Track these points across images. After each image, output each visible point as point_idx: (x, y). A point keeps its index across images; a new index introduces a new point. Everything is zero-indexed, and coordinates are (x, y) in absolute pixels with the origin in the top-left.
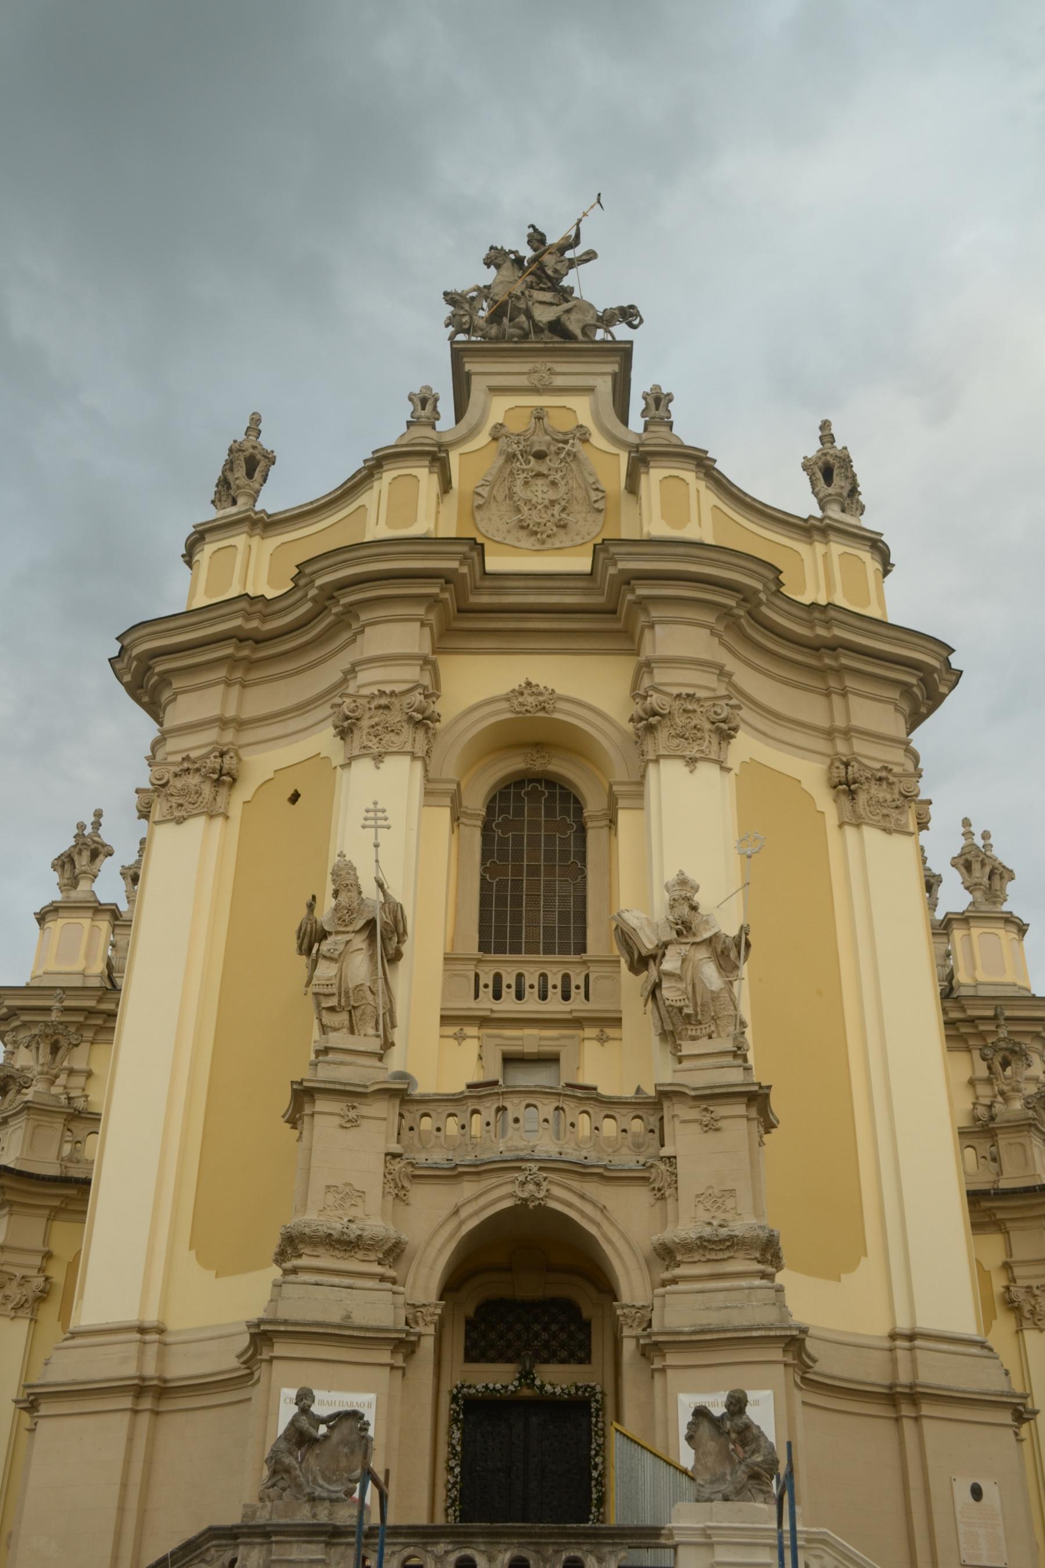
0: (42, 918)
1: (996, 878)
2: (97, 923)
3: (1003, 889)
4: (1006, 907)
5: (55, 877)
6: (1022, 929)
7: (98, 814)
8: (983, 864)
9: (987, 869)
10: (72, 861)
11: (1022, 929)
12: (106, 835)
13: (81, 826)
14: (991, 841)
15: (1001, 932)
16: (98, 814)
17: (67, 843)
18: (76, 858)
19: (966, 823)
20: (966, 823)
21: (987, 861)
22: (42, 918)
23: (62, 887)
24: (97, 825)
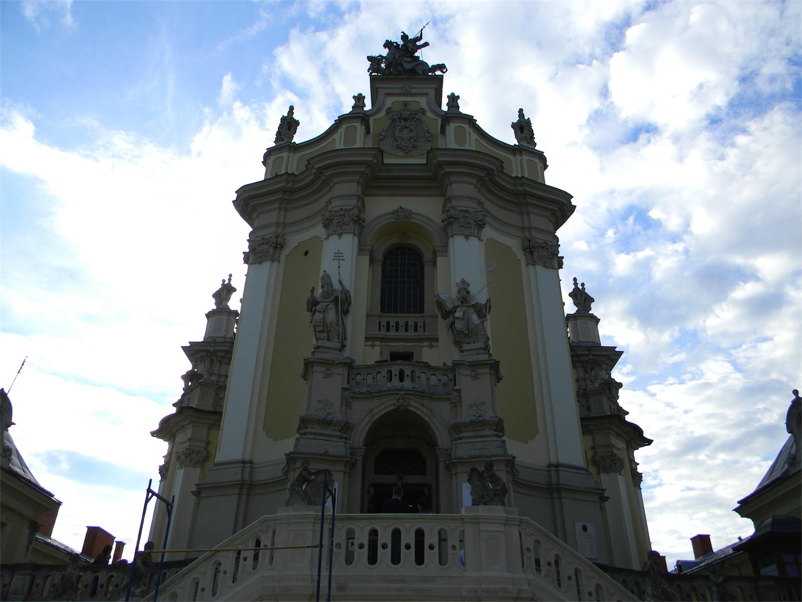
0: (208, 316)
1: (587, 301)
2: (230, 318)
4: (590, 312)
5: (214, 300)
6: (598, 320)
7: (230, 276)
8: (582, 295)
9: (583, 298)
11: (598, 320)
12: (233, 284)
13: (224, 281)
15: (589, 322)
16: (230, 276)
17: (218, 286)
18: (222, 293)
19: (575, 279)
20: (575, 279)
21: (583, 294)
23: (216, 304)
24: (230, 280)
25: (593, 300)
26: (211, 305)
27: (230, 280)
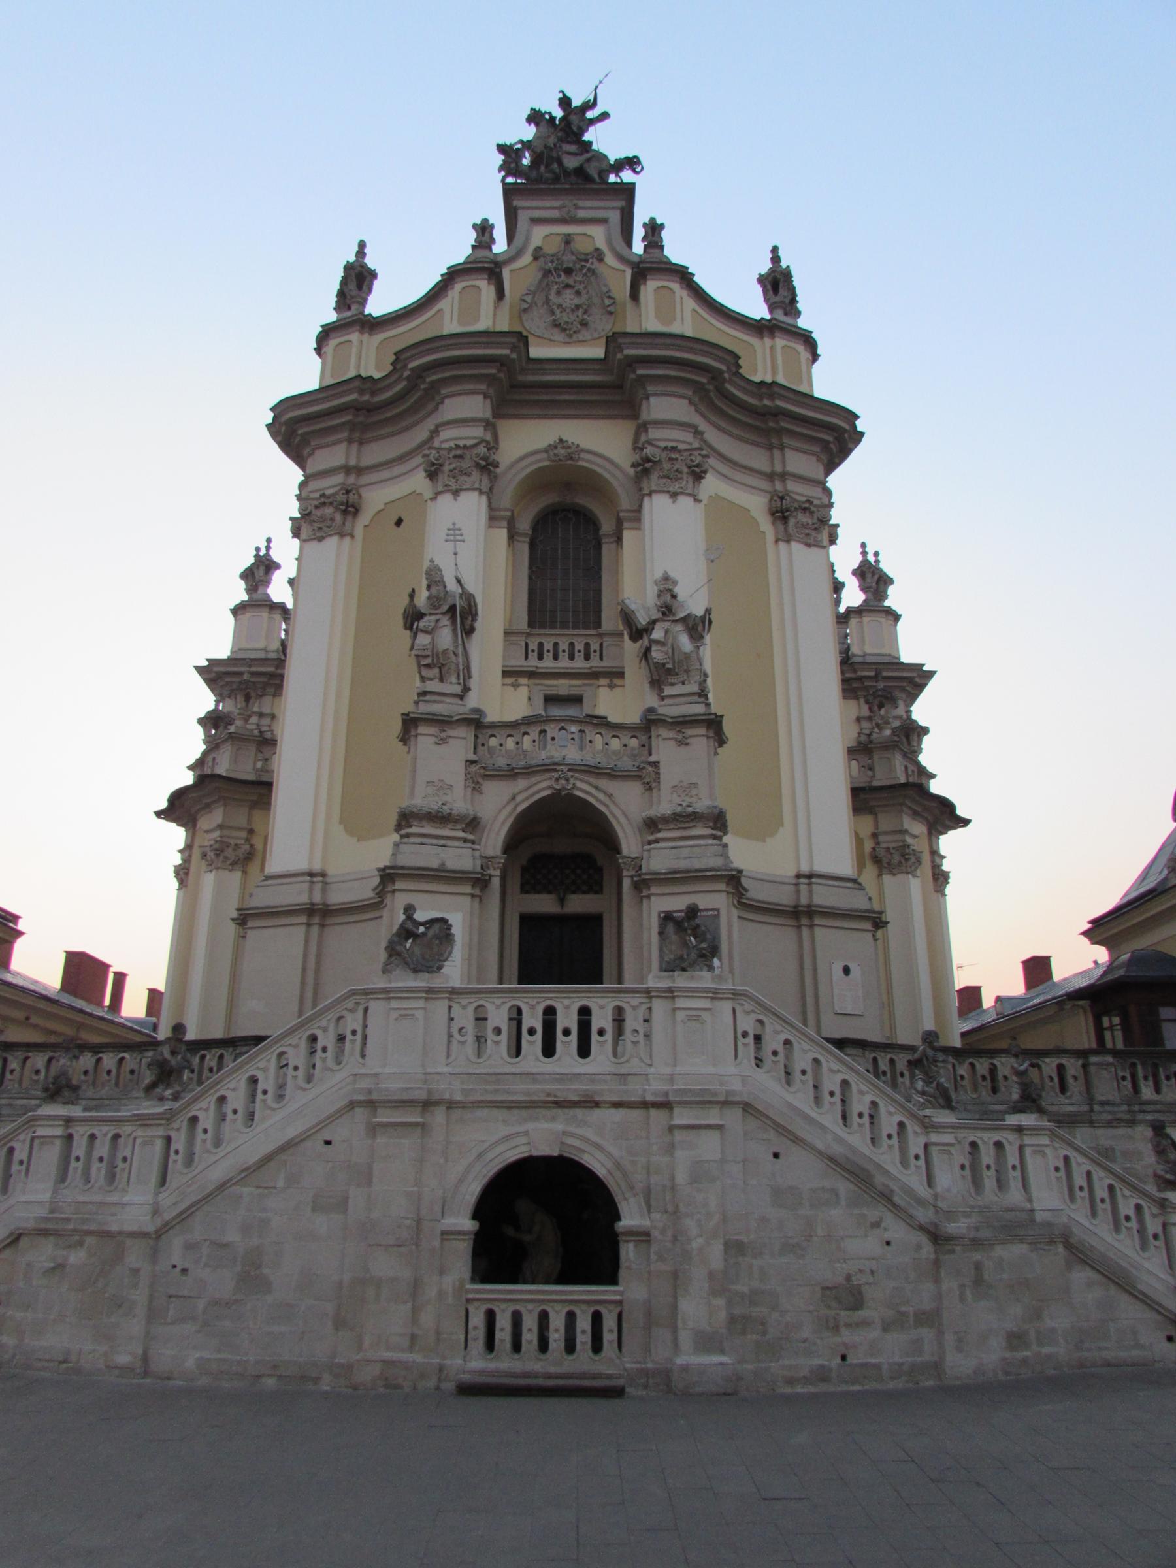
1: (882, 583)
3: (885, 591)
4: (886, 603)
5: (242, 585)
6: (896, 617)
7: (269, 540)
8: (873, 574)
9: (876, 577)
10: (253, 573)
11: (896, 617)
12: (275, 555)
13: (258, 549)
14: (880, 558)
15: (883, 620)
16: (269, 540)
18: (255, 571)
19: (863, 545)
20: (863, 545)
22: (237, 611)
23: (248, 591)
24: (268, 548)
25: (889, 581)
26: (240, 594)
27: (268, 548)
